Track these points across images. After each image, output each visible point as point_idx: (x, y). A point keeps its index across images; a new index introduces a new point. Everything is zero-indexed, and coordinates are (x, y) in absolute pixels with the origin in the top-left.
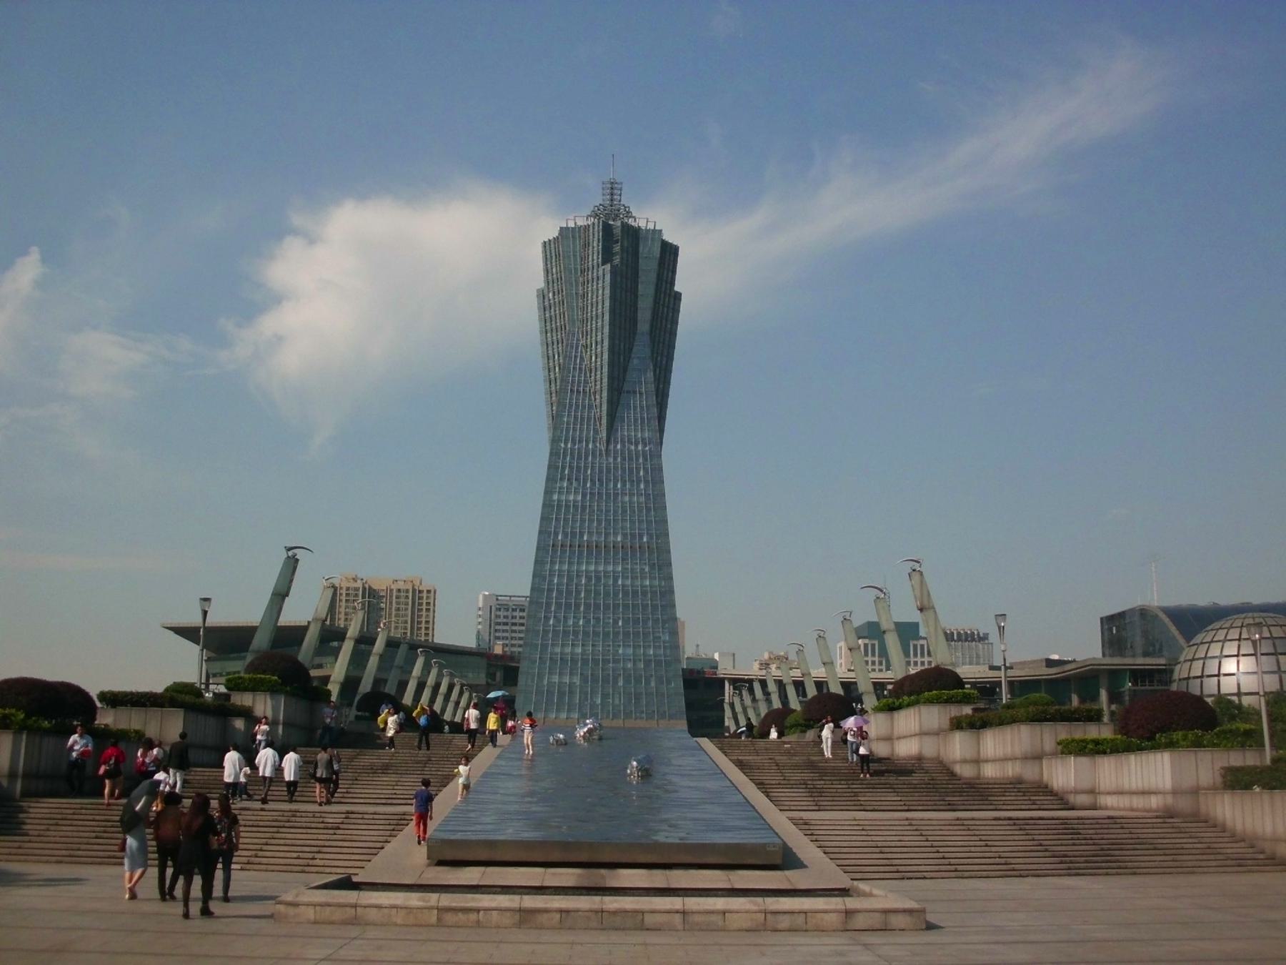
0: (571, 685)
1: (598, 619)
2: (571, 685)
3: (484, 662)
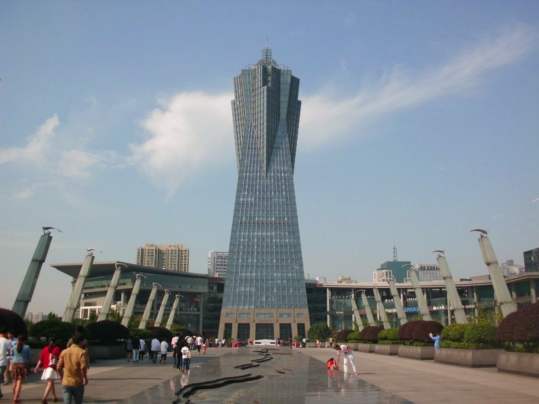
0: (250, 292)
1: (263, 259)
2: (250, 292)
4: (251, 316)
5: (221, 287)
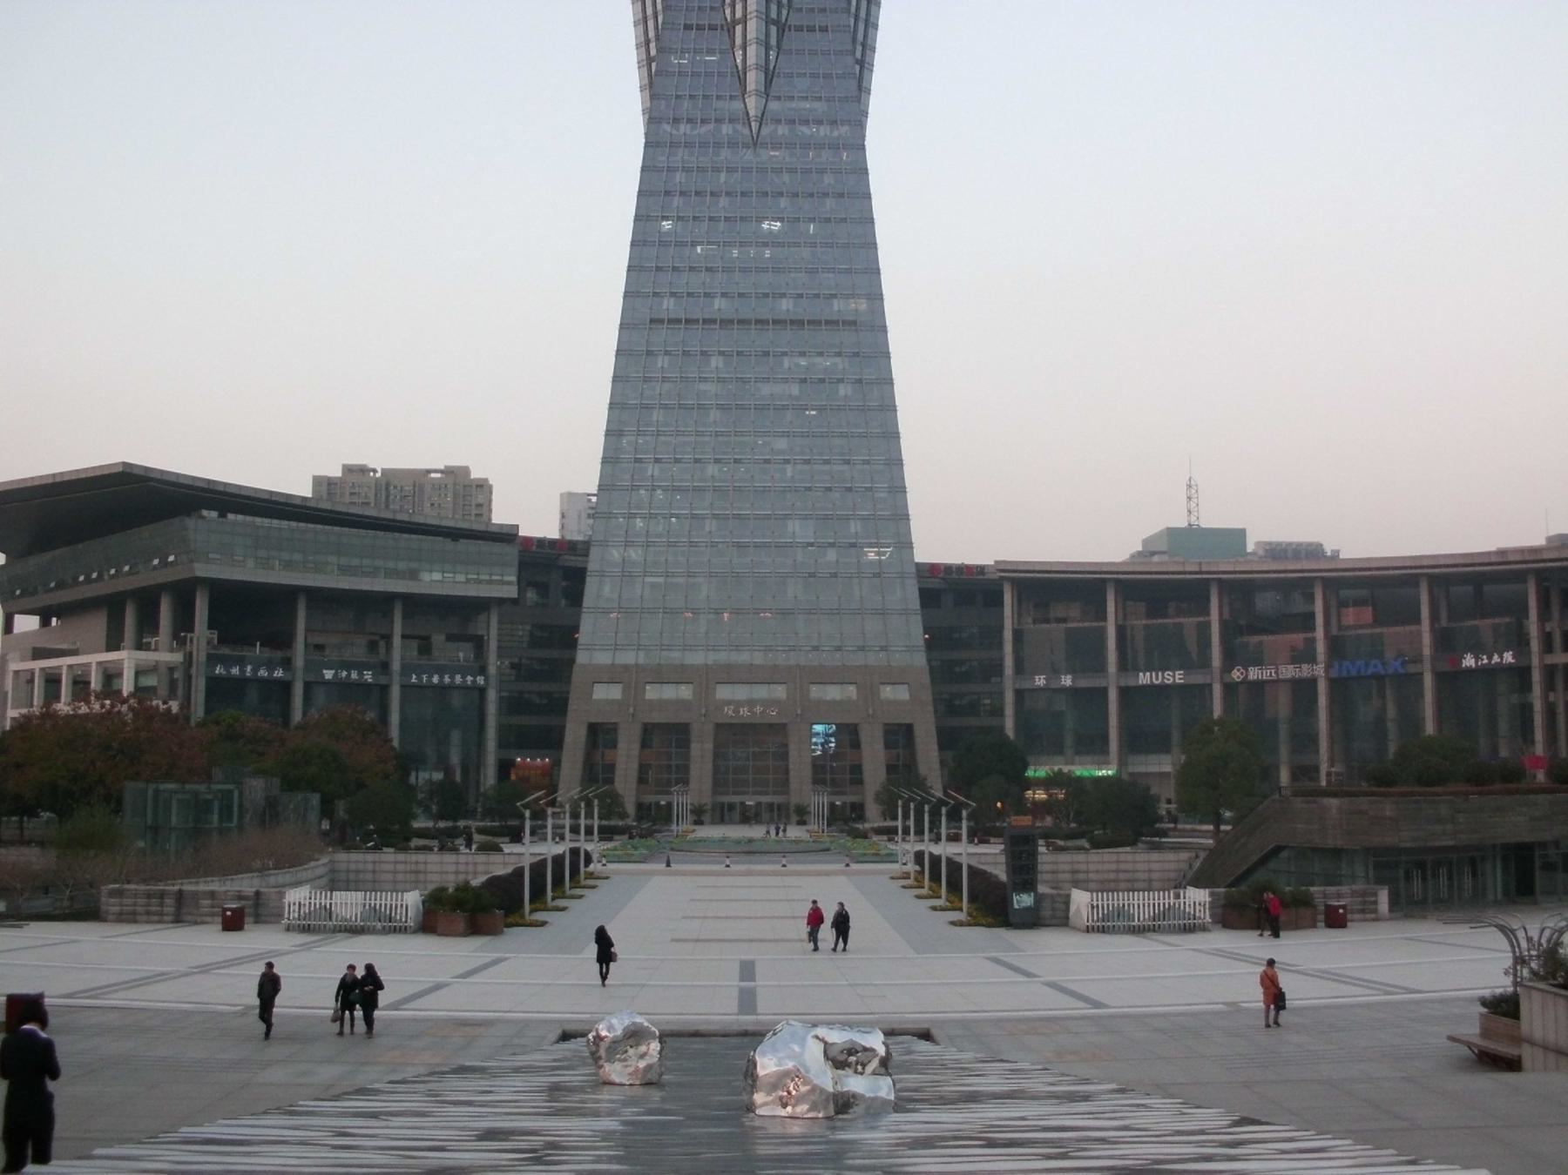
3: (512, 552)
5: (576, 579)
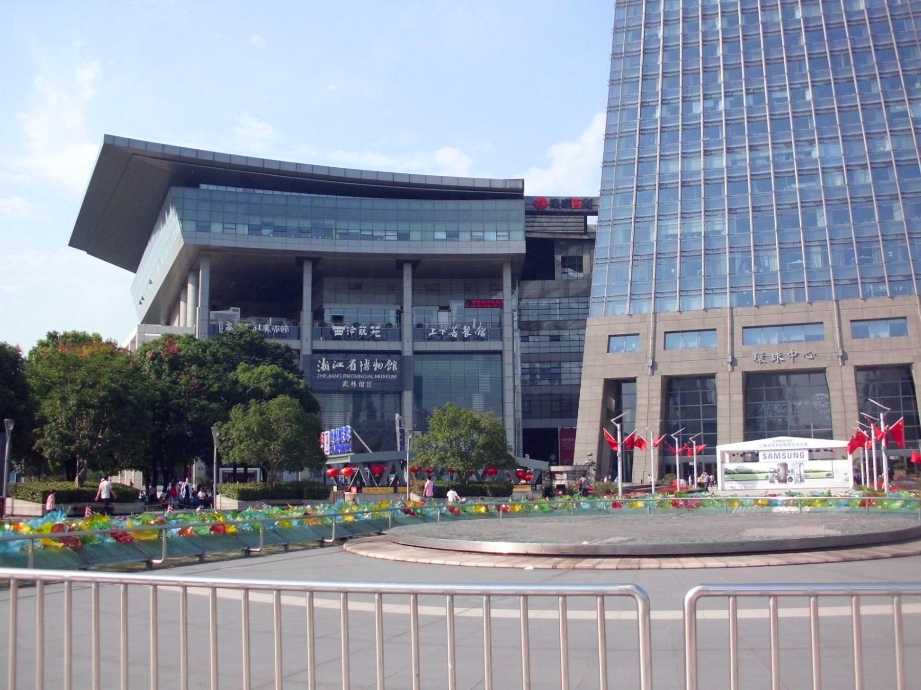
4: (720, 343)
